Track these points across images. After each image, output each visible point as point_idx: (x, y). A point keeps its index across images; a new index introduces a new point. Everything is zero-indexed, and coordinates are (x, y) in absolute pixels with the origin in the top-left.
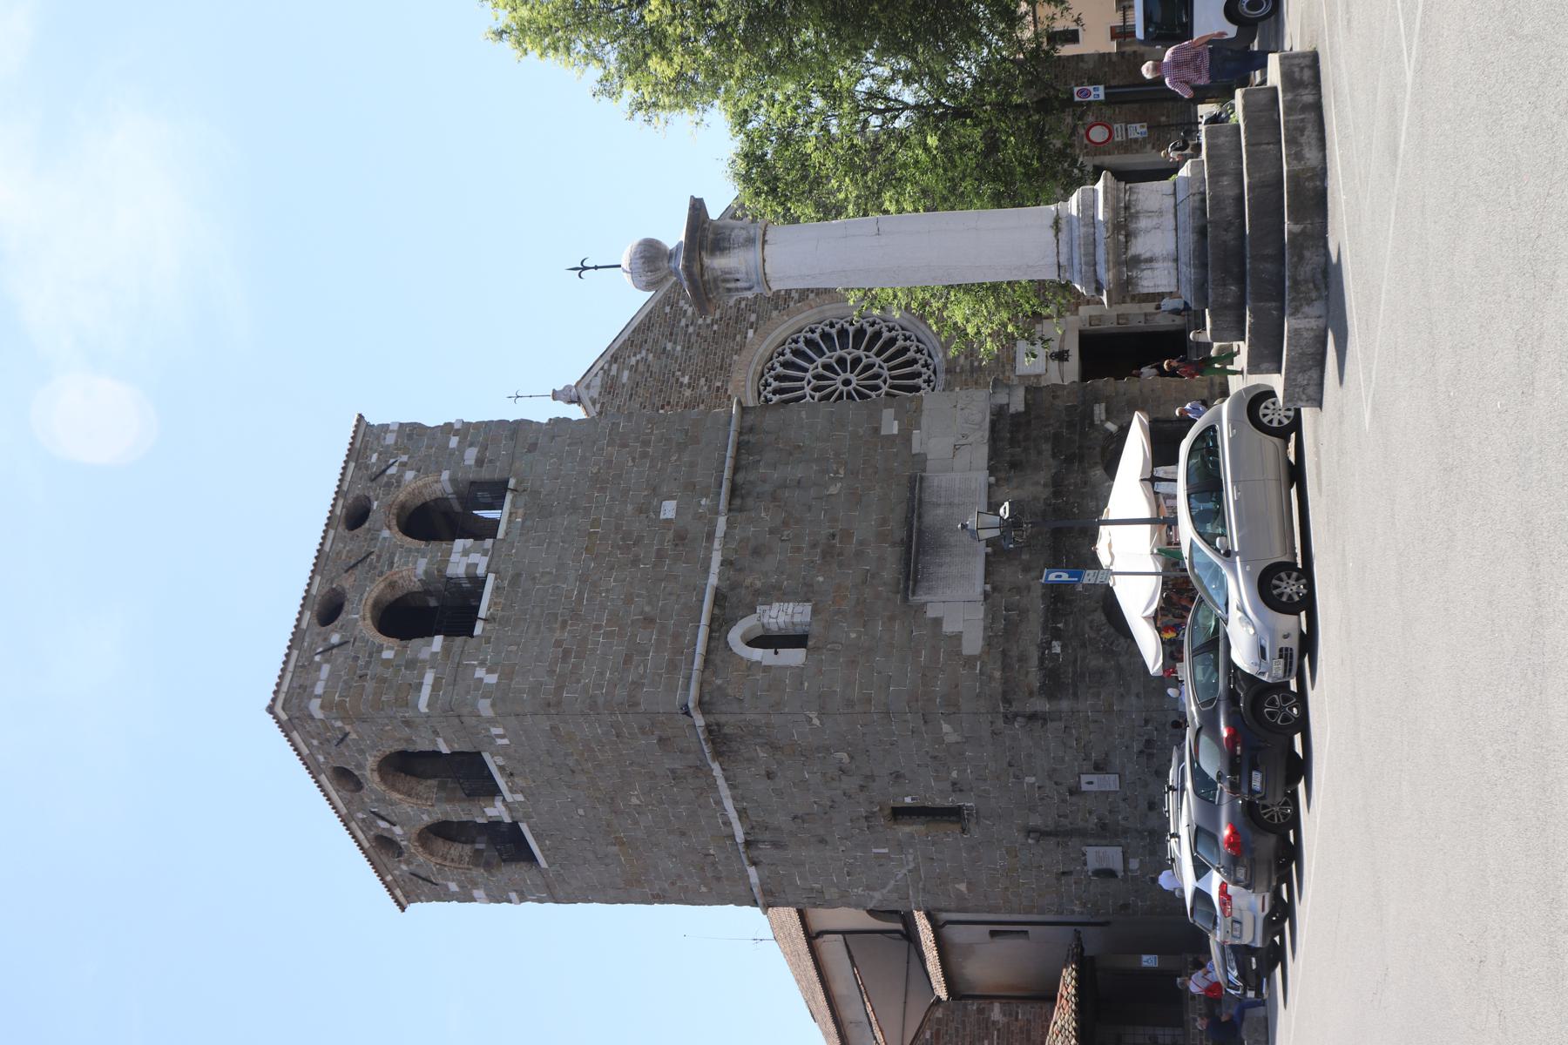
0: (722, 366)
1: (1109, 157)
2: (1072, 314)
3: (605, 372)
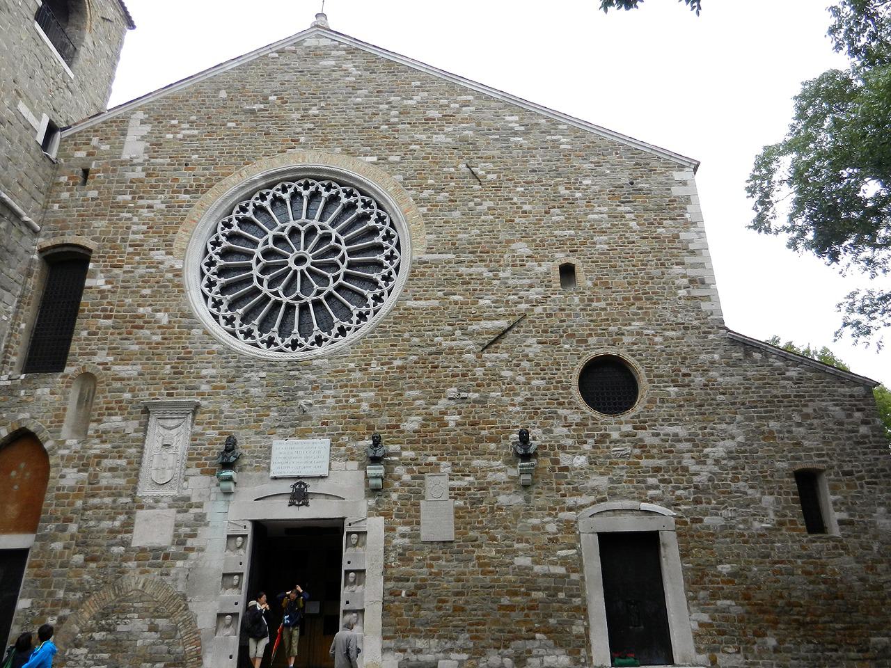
1: (677, 553)
2: (371, 508)
3: (335, 47)
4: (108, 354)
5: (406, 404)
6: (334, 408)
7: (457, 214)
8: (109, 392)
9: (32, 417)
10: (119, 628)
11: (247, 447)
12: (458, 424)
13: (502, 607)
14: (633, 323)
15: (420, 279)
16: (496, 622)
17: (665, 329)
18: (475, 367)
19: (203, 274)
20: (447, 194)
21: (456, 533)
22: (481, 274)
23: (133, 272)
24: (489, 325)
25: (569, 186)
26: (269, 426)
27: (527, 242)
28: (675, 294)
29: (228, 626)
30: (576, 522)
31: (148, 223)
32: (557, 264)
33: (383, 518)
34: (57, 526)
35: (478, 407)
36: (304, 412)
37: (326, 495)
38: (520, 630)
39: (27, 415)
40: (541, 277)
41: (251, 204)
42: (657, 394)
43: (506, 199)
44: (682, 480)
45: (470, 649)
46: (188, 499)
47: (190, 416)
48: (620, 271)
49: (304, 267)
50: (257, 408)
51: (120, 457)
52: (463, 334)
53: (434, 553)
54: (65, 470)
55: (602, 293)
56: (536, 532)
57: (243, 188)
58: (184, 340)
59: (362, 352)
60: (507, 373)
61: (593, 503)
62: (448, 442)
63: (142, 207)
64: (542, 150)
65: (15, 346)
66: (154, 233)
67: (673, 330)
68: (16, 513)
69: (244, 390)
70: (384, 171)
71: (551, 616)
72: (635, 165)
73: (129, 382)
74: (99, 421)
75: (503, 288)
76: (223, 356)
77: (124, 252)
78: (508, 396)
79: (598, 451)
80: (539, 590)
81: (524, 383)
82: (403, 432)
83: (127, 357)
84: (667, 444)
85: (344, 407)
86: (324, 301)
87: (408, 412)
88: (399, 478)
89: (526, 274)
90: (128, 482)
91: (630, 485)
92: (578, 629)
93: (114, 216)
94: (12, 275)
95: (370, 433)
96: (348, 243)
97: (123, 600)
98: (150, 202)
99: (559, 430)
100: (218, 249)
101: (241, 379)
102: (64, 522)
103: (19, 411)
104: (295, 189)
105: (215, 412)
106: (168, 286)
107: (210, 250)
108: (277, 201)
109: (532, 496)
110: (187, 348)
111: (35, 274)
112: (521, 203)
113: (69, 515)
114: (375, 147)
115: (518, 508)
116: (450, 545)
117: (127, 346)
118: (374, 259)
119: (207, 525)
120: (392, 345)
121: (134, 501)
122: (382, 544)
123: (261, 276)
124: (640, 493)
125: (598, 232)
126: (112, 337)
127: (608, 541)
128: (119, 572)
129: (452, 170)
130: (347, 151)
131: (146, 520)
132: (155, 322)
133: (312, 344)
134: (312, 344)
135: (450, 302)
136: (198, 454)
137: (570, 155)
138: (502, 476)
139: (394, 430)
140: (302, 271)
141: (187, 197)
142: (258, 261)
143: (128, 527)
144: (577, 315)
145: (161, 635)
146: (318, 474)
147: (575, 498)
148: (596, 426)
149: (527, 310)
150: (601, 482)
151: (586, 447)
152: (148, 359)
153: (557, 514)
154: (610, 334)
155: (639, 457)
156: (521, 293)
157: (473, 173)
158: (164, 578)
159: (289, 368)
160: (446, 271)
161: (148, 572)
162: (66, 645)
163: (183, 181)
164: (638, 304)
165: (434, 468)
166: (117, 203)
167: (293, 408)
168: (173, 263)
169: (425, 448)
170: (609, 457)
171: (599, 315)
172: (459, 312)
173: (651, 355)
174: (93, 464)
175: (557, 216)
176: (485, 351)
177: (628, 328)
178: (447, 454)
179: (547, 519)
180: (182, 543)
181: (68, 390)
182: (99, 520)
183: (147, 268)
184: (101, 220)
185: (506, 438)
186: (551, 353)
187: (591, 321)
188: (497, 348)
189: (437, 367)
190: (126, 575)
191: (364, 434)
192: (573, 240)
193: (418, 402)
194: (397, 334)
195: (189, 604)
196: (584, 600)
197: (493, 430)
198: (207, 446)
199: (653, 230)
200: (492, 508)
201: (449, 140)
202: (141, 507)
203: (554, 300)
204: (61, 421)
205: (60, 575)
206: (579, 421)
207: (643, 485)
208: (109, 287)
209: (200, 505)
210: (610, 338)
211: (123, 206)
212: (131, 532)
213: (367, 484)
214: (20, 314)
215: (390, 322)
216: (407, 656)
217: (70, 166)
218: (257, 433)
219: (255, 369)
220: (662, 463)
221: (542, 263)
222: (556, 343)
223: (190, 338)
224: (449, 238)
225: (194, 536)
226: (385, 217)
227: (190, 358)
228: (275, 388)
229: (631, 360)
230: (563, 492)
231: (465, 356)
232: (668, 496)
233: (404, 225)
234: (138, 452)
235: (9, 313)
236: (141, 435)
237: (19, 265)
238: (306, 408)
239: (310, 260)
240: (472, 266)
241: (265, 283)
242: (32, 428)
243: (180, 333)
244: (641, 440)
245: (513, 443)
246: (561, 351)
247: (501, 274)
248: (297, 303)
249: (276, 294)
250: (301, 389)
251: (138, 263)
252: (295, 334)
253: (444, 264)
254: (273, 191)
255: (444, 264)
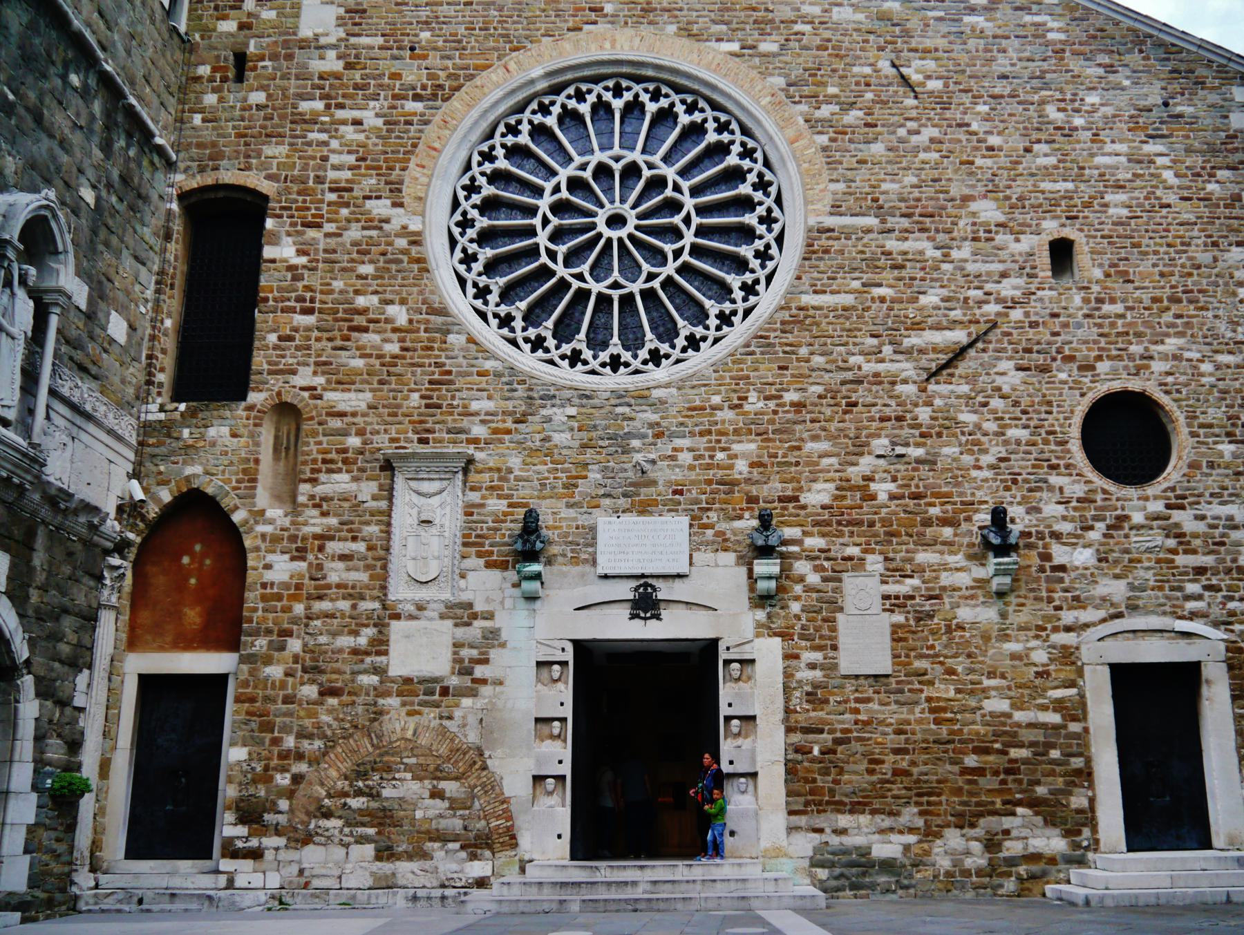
0: (655, 9)
2: (759, 625)
4: (315, 373)
5: (808, 464)
6: (691, 468)
7: (878, 149)
8: (324, 435)
9: (207, 473)
10: (386, 793)
11: (556, 528)
12: (893, 497)
13: (966, 771)
14: (1167, 340)
15: (821, 259)
16: (958, 791)
17: (1216, 352)
18: (916, 405)
19: (453, 242)
20: (860, 114)
21: (894, 664)
22: (921, 253)
23: (340, 235)
24: (938, 338)
25: (1062, 105)
26: (587, 494)
27: (996, 200)
28: (1234, 294)
29: (550, 793)
30: (1077, 648)
31: (357, 152)
32: (1046, 238)
33: (779, 639)
34: (271, 642)
35: (924, 470)
36: (643, 472)
37: (687, 603)
38: (993, 803)
39: (197, 469)
40: (1021, 259)
41: (525, 122)
42: (1203, 455)
43: (959, 125)
44: (1238, 587)
45: (919, 829)
46: (470, 605)
47: (460, 476)
48: (1146, 253)
49: (623, 233)
50: (566, 465)
51: (354, 539)
52: (895, 352)
53: (861, 692)
54: (270, 558)
55: (1118, 288)
56: (1017, 663)
57: (513, 92)
58: (436, 352)
59: (732, 378)
60: (968, 418)
61: (1104, 620)
62: (878, 525)
63: (344, 122)
64: (1016, 42)
65: (160, 356)
66: (368, 168)
67: (1230, 353)
68: (198, 620)
69: (542, 436)
70: (753, 68)
71: (1038, 783)
72: (1171, 72)
73: (355, 420)
74: (314, 481)
75: (959, 277)
76: (504, 379)
77: (322, 201)
78: (970, 452)
79: (1111, 541)
80: (1021, 746)
81: (997, 434)
82: (804, 507)
83: (346, 379)
84: (1217, 532)
85: (709, 467)
86: (661, 293)
87: (812, 476)
88: (801, 579)
89: (996, 255)
90: (372, 577)
91: (1160, 594)
92: (1078, 801)
93: (296, 137)
94: (147, 238)
95: (752, 509)
96: (695, 192)
97: (387, 753)
98: (357, 114)
99: (1052, 509)
100: (476, 199)
101: (537, 418)
102: (279, 635)
103: (185, 463)
104: (599, 97)
105: (499, 470)
106: (401, 261)
107: (462, 199)
108: (570, 117)
109: (1011, 609)
110: (444, 365)
111: (175, 236)
112: (986, 132)
113: (286, 626)
114: (734, 26)
115: (988, 627)
116: (882, 679)
117: (344, 360)
118: (740, 223)
119: (503, 645)
120: (780, 368)
121: (385, 607)
122: (780, 678)
123: (552, 246)
124: (1174, 606)
125: (1112, 186)
126: (319, 345)
127: (1124, 676)
128: (375, 713)
129: (868, 70)
130: (687, 32)
131: (407, 637)
132: (387, 321)
133: (645, 362)
134: (645, 362)
135: (873, 299)
136: (478, 536)
137: (1063, 51)
138: (963, 579)
139: (791, 505)
140: (620, 240)
141: (418, 106)
142: (546, 222)
143: (380, 645)
144: (1079, 326)
145: (451, 804)
146: (674, 571)
147: (1075, 613)
148: (1108, 503)
149: (998, 314)
150: (1117, 589)
151: (1094, 535)
152: (381, 382)
153: (1048, 636)
154: (1131, 358)
155: (1174, 552)
156: (989, 287)
157: (902, 76)
158: (446, 723)
159: (613, 402)
160: (864, 246)
161: (419, 713)
162: (310, 815)
163: (409, 78)
164: (1175, 308)
165: (857, 564)
166: (300, 114)
167: (625, 466)
168: (405, 221)
169: (841, 534)
170: (1127, 551)
171: (1113, 325)
172: (888, 316)
173: (1195, 392)
174: (312, 550)
175: (1044, 157)
176: (932, 380)
177: (1160, 348)
178: (877, 543)
179: (1033, 643)
180: (469, 672)
181: (258, 429)
182: (334, 634)
183: (364, 228)
184: (277, 144)
185: (968, 519)
186: (1037, 386)
187: (1101, 335)
188: (952, 375)
189: (855, 404)
190: (386, 717)
191: (741, 509)
192: (1071, 198)
193: (826, 462)
194: (788, 349)
195: (489, 762)
196: (1088, 761)
197: (949, 507)
198: (491, 524)
199: (1200, 185)
200: (948, 627)
201: (860, 17)
202: (397, 617)
203: (1041, 300)
204: (254, 480)
205: (285, 715)
206: (1082, 495)
207: (1179, 594)
208: (303, 260)
209: (489, 616)
210: (1131, 364)
211: (311, 121)
212: (386, 653)
213: (752, 589)
214: (162, 303)
215: (775, 330)
216: (824, 838)
217: (212, 48)
218: (569, 506)
219: (558, 402)
220: (1209, 560)
221: (1022, 237)
222: (1044, 369)
223: (447, 349)
224: (867, 190)
225: (485, 661)
226: (754, 150)
227: (451, 382)
228: (594, 434)
229: (1164, 400)
230: (1057, 603)
231: (900, 388)
232: (1216, 612)
233: (792, 166)
234: (382, 531)
235: (147, 301)
236: (383, 504)
237: (153, 221)
238: (647, 467)
239: (632, 222)
240: (906, 239)
241: (560, 258)
242: (210, 490)
243: (429, 340)
244: (1177, 525)
245: (980, 528)
246: (1053, 382)
247: (955, 254)
248: (616, 294)
249: (580, 277)
250: (635, 436)
251: (348, 221)
252: (615, 346)
253: (860, 234)
254: (561, 99)
255: (860, 234)
